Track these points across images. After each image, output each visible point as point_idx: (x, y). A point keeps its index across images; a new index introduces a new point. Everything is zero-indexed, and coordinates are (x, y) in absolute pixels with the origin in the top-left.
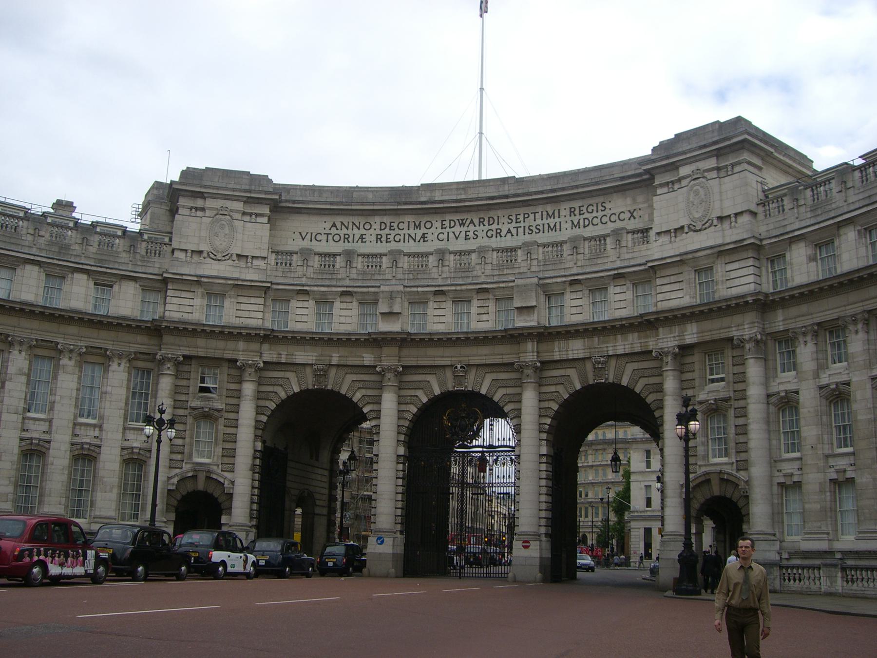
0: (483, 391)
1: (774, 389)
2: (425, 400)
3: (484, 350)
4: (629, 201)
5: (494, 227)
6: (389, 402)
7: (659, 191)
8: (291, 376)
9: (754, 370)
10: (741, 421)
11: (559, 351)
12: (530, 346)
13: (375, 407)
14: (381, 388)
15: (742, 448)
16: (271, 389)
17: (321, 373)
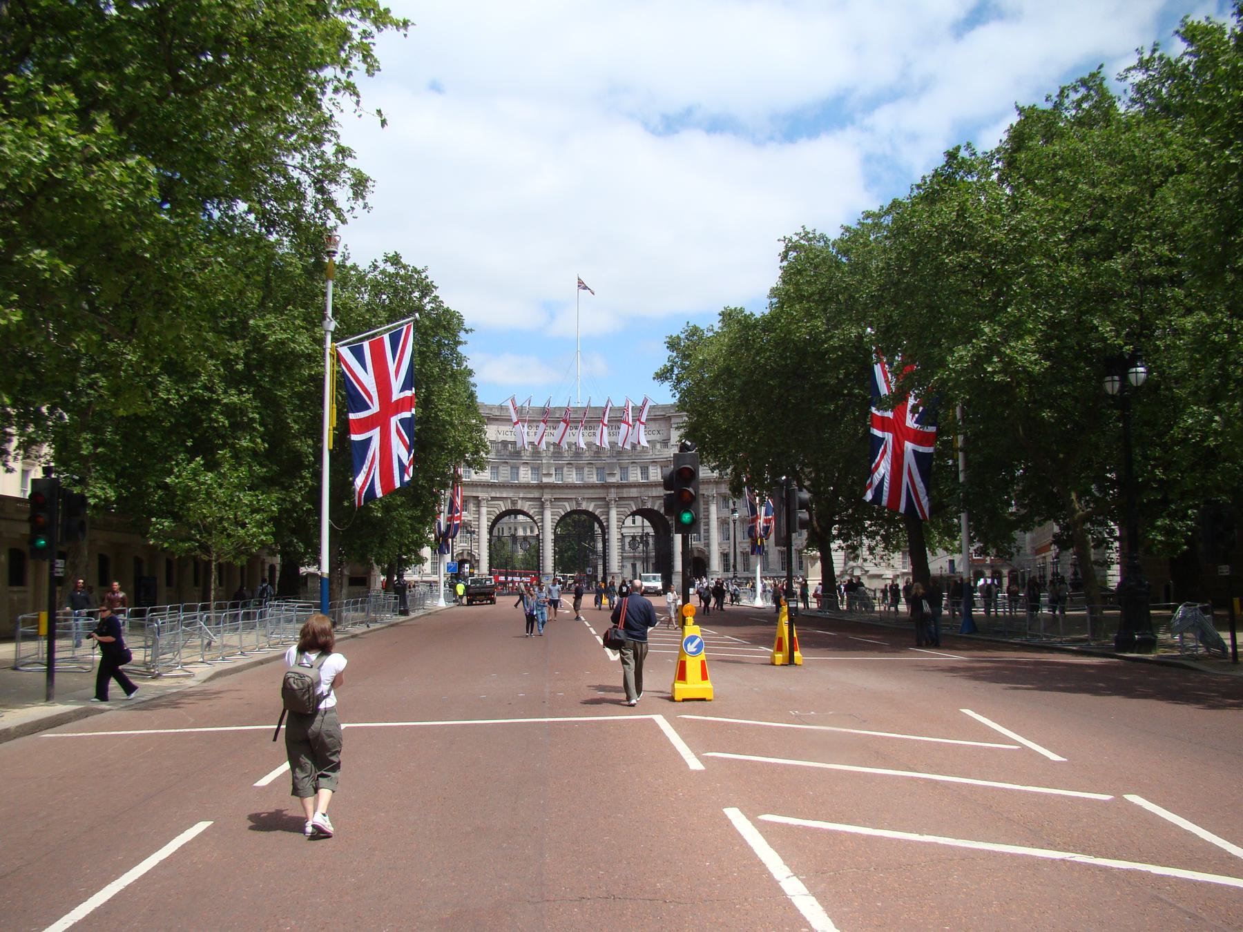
0: (590, 510)
1: (720, 516)
2: (563, 514)
3: (591, 491)
4: (657, 425)
5: (592, 431)
6: (548, 514)
7: (673, 426)
8: (501, 503)
9: (713, 509)
10: (706, 527)
11: (626, 493)
12: (613, 490)
13: (540, 517)
14: (542, 507)
15: (707, 538)
16: (492, 509)
17: (514, 503)
